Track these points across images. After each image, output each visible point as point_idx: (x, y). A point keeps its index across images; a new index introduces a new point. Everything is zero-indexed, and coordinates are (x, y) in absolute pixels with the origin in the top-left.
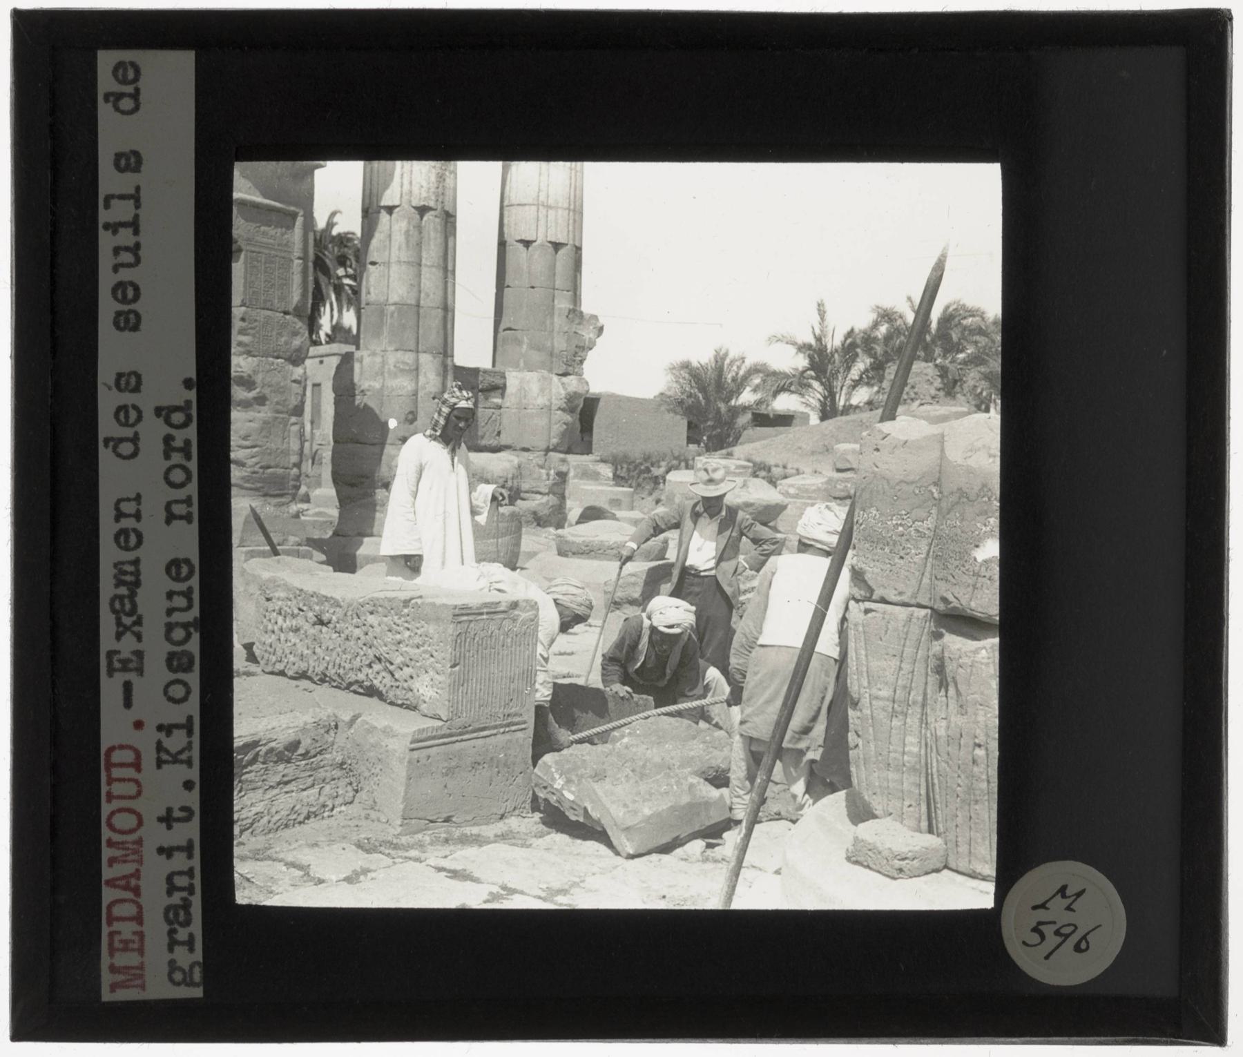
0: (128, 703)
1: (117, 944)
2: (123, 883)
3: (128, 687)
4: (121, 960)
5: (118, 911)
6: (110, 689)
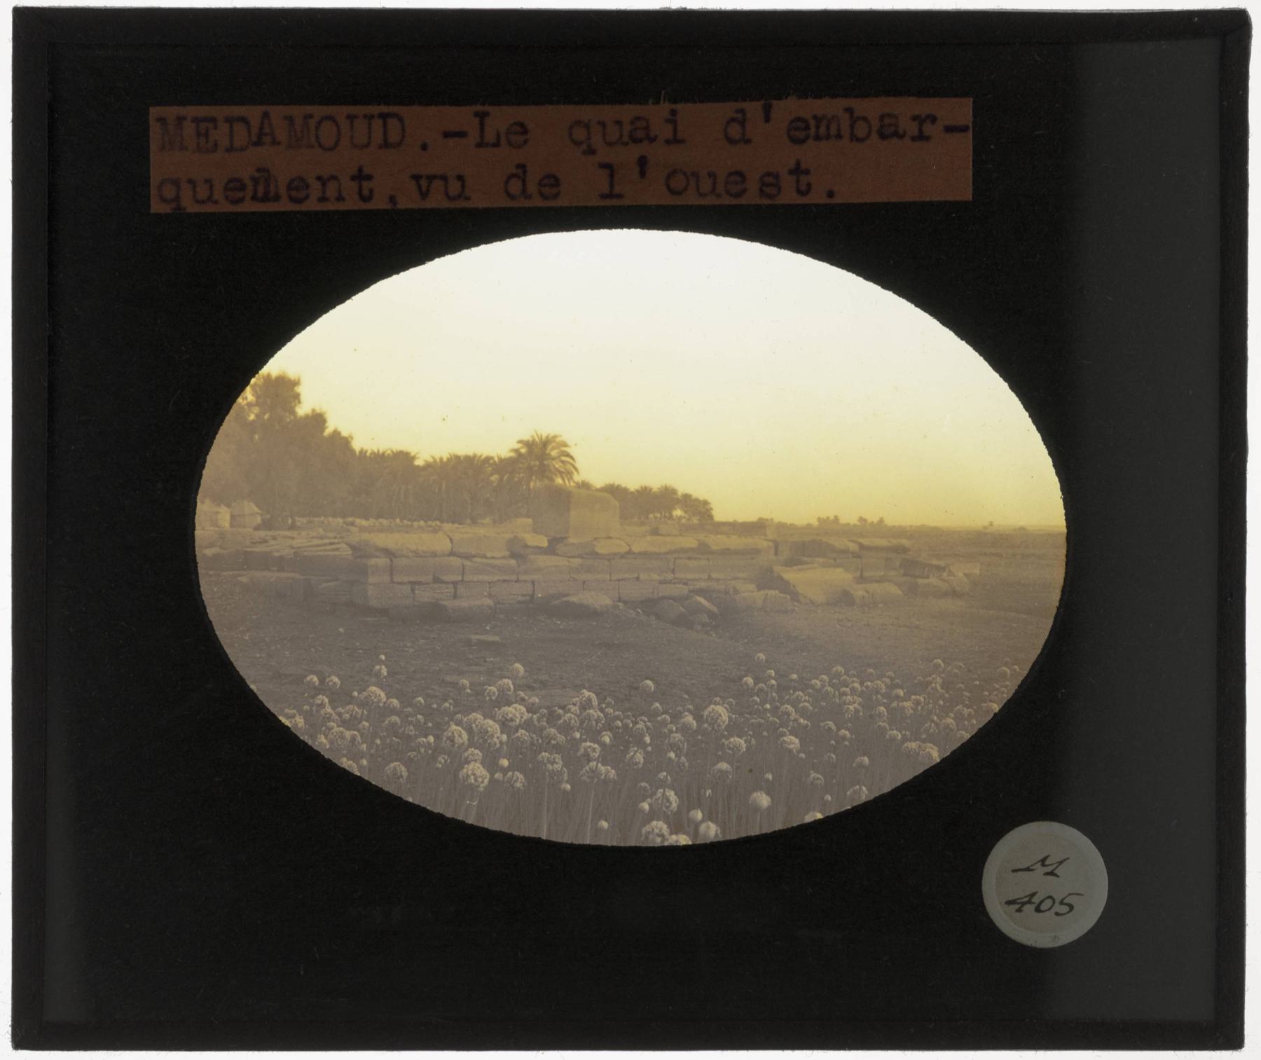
0: (447, 135)
1: (203, 126)
2: (267, 130)
3: (461, 134)
4: (189, 129)
5: (239, 128)
6: (461, 116)
